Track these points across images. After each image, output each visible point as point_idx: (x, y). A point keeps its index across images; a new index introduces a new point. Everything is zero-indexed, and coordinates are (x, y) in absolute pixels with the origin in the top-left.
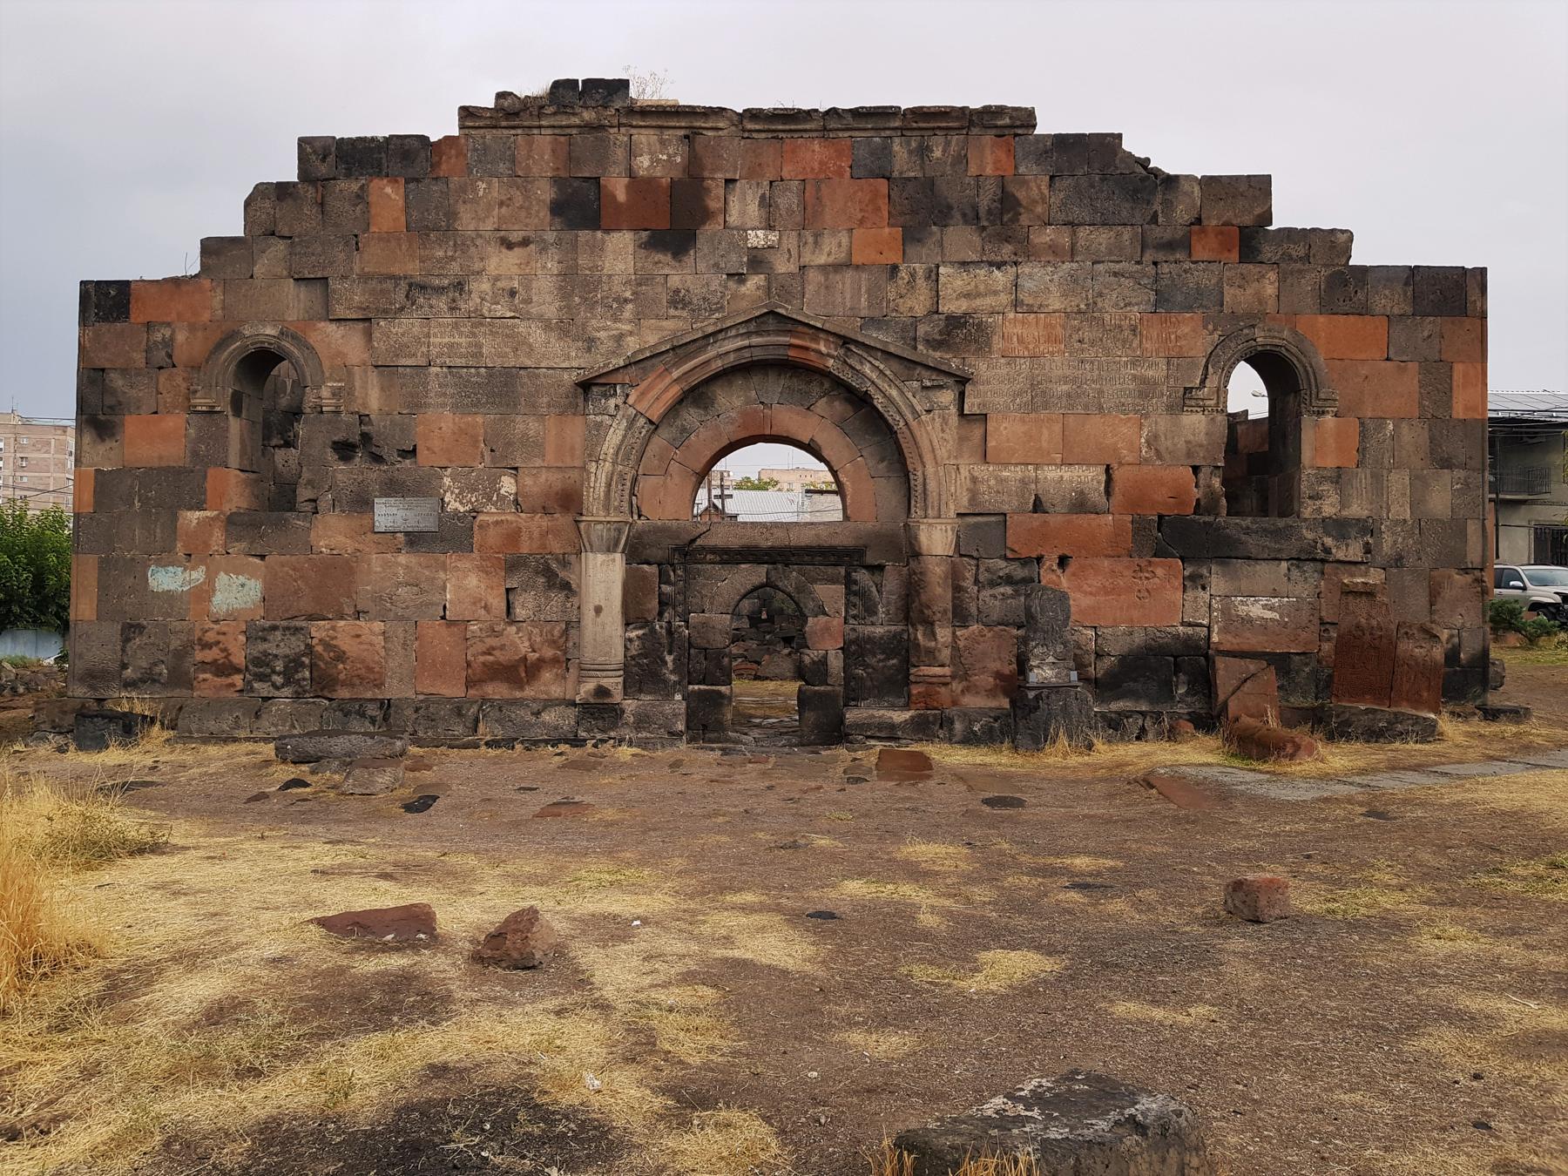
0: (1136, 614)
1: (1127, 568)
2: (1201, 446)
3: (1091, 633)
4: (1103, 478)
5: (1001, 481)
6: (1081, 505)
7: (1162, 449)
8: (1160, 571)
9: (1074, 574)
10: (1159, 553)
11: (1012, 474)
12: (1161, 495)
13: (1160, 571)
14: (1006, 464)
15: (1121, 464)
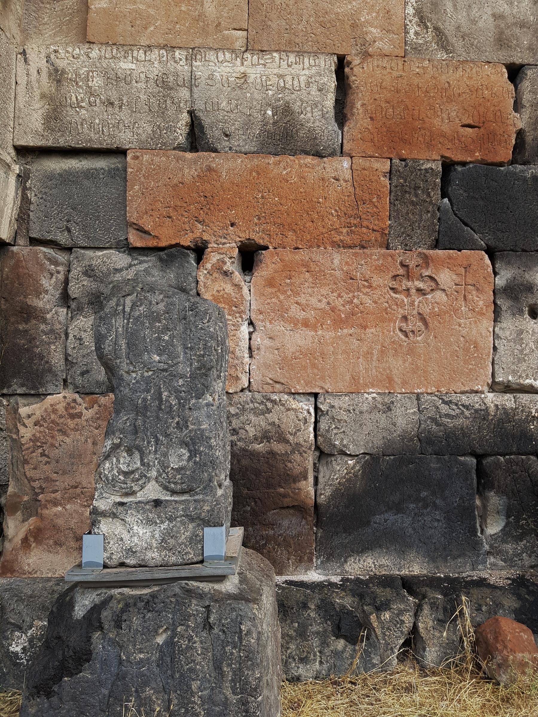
0: (397, 365)
1: (379, 269)
2: (523, 25)
3: (306, 406)
4: (331, 82)
5: (116, 79)
6: (284, 137)
7: (449, 28)
8: (446, 277)
9: (270, 283)
10: (446, 239)
11: (140, 66)
12: (447, 120)
13: (446, 277)
14: (126, 47)
15: (366, 55)
